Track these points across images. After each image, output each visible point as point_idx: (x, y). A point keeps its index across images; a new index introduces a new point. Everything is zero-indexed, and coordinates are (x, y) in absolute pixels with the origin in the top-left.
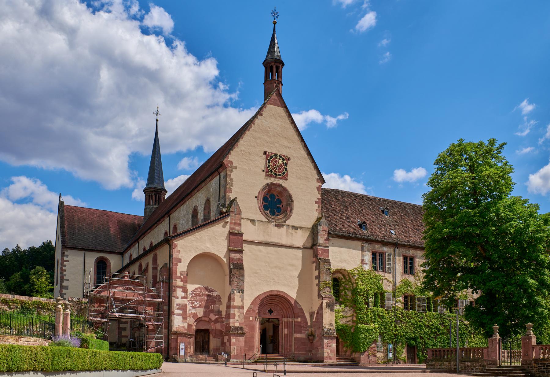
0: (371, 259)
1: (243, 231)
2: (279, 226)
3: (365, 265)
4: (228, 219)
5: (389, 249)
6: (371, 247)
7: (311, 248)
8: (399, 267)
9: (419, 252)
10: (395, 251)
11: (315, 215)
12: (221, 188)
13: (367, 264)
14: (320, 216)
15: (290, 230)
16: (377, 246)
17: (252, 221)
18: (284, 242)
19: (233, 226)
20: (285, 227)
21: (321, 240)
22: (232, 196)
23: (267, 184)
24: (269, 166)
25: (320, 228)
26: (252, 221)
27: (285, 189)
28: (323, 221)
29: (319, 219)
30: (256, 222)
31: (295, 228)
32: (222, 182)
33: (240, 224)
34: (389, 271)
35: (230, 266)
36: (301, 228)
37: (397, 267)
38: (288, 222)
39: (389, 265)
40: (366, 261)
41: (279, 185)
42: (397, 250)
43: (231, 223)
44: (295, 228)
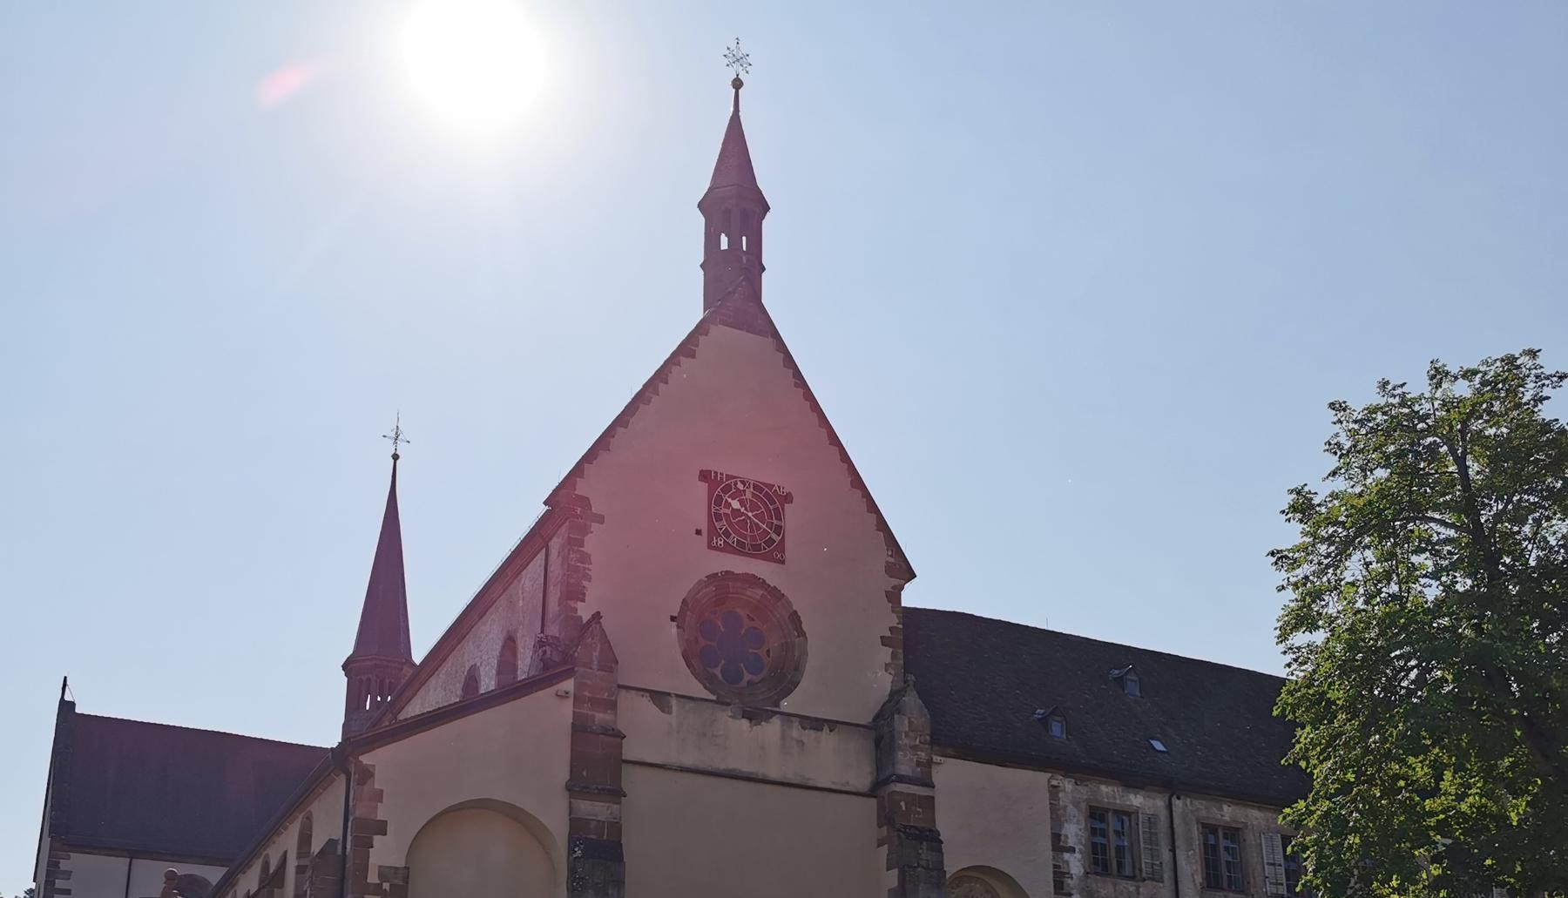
0: (1084, 835)
1: (621, 727)
2: (754, 716)
3: (1067, 856)
4: (568, 685)
5: (1150, 802)
6: (1084, 792)
7: (872, 793)
8: (1191, 869)
9: (1255, 813)
10: (1170, 807)
11: (882, 682)
12: (551, 588)
13: (1072, 850)
14: (901, 684)
15: (796, 731)
16: (1104, 788)
17: (659, 698)
18: (774, 774)
19: (585, 710)
20: (776, 722)
21: (905, 764)
22: (584, 612)
23: (713, 577)
24: (719, 517)
25: (901, 724)
26: (659, 698)
27: (776, 594)
28: (911, 700)
29: (895, 695)
30: (674, 702)
31: (815, 724)
32: (556, 568)
33: (612, 706)
34: (1156, 877)
35: (571, 851)
36: (833, 725)
37: (1181, 861)
38: (785, 705)
39: (1154, 853)
40: (1071, 842)
41: (753, 580)
42: (1178, 804)
43: (578, 700)
44: (815, 724)
